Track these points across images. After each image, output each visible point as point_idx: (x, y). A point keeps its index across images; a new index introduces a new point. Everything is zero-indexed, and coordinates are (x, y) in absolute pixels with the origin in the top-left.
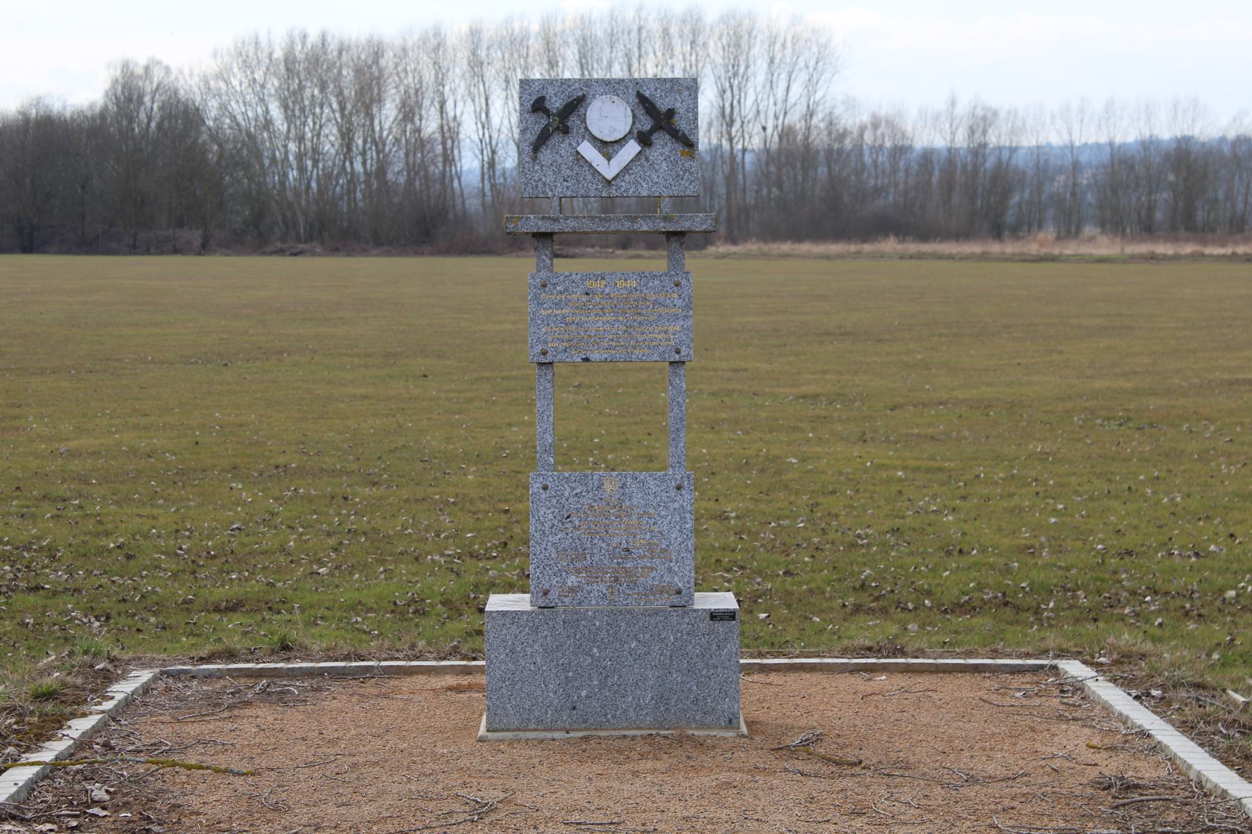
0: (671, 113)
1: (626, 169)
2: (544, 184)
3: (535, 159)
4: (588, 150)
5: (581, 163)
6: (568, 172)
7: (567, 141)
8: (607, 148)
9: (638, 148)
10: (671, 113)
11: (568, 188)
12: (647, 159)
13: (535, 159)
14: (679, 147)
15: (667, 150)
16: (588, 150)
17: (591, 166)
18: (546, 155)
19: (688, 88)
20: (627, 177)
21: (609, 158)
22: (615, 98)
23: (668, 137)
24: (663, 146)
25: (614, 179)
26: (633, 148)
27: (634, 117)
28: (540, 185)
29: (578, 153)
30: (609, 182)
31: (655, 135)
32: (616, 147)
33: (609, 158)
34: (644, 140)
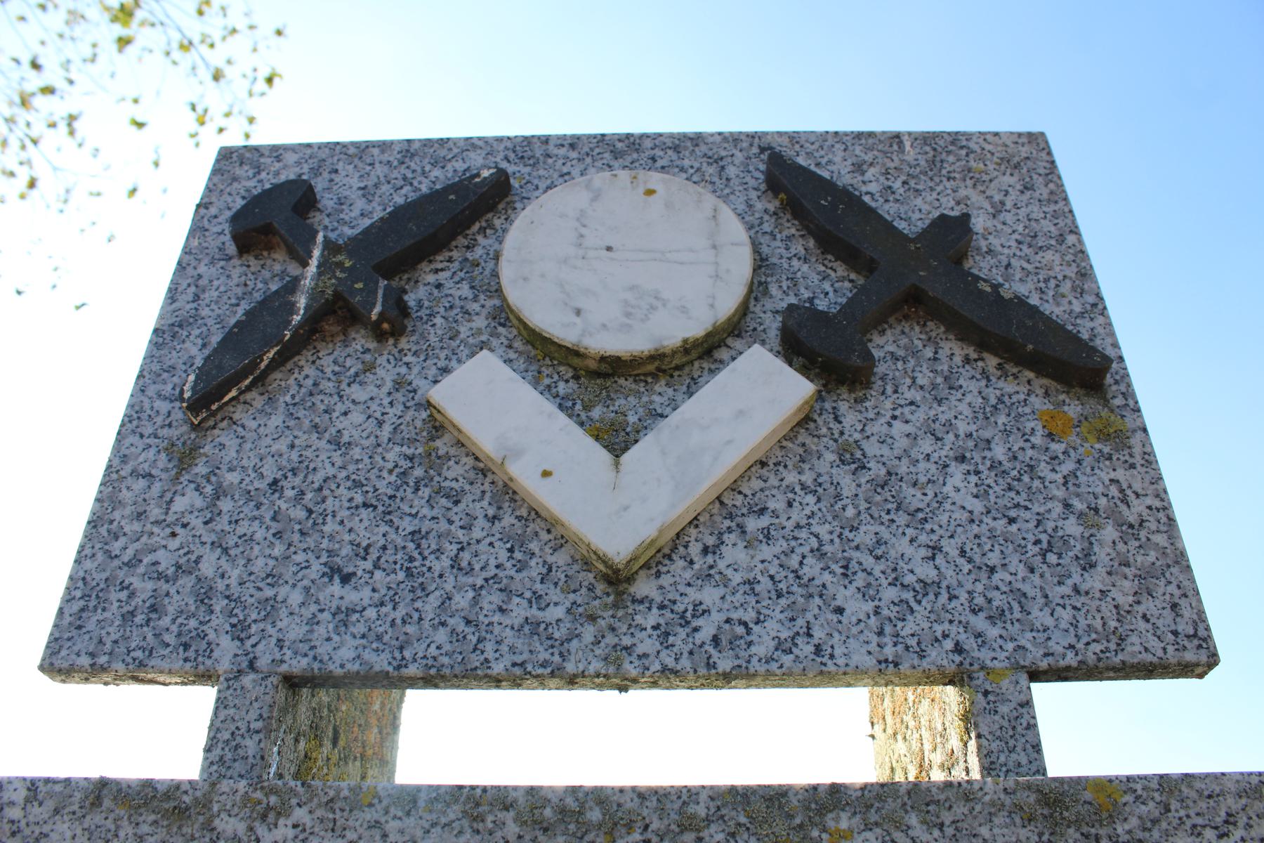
0: (952, 233)
1: (729, 508)
2: (204, 596)
3: (184, 458)
4: (488, 400)
5: (456, 472)
6: (366, 529)
7: (387, 372)
8: (612, 389)
9: (796, 388)
10: (952, 233)
11: (344, 616)
12: (851, 457)
13: (184, 458)
14: (1031, 397)
15: (961, 410)
16: (488, 400)
17: (508, 493)
18: (259, 437)
19: (1011, 164)
20: (734, 553)
21: (616, 440)
22: (655, 179)
23: (953, 350)
24: (930, 395)
25: (657, 557)
26: (761, 392)
27: (761, 263)
28: (181, 595)
29: (437, 425)
30: (616, 579)
31: (883, 345)
32: (660, 393)
33: (616, 440)
34: (829, 355)
